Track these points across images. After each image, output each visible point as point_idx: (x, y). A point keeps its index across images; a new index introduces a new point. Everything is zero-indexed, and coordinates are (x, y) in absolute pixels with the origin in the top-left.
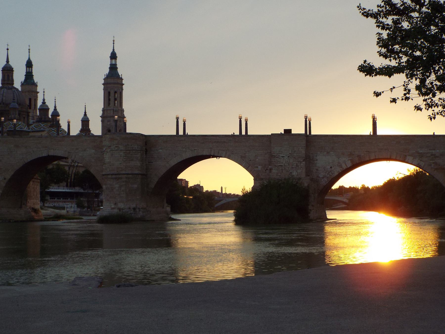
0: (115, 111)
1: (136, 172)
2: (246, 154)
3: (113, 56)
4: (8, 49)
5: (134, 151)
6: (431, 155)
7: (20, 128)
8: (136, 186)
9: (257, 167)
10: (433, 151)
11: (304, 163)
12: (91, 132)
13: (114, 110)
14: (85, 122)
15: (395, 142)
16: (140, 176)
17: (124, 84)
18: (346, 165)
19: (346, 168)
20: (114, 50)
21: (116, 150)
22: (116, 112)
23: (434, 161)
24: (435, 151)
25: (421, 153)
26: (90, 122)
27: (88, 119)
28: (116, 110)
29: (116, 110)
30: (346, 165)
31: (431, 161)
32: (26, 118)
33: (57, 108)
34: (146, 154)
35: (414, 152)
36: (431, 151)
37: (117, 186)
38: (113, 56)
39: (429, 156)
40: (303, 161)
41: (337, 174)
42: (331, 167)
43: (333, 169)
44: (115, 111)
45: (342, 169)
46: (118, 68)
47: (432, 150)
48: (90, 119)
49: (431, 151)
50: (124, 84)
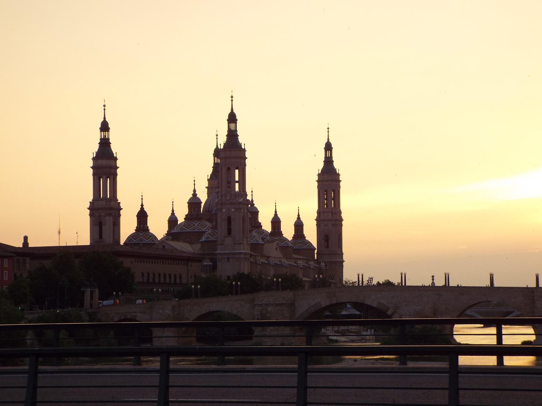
0: (334, 213)
3: (328, 147)
7: (255, 241)
12: (306, 238)
13: (332, 212)
14: (299, 226)
17: (341, 181)
20: (328, 139)
22: (335, 214)
26: (304, 226)
27: (302, 223)
28: (335, 212)
29: (335, 212)
33: (300, 217)
38: (328, 147)
44: (334, 213)
46: (334, 162)
48: (304, 224)
50: (341, 181)
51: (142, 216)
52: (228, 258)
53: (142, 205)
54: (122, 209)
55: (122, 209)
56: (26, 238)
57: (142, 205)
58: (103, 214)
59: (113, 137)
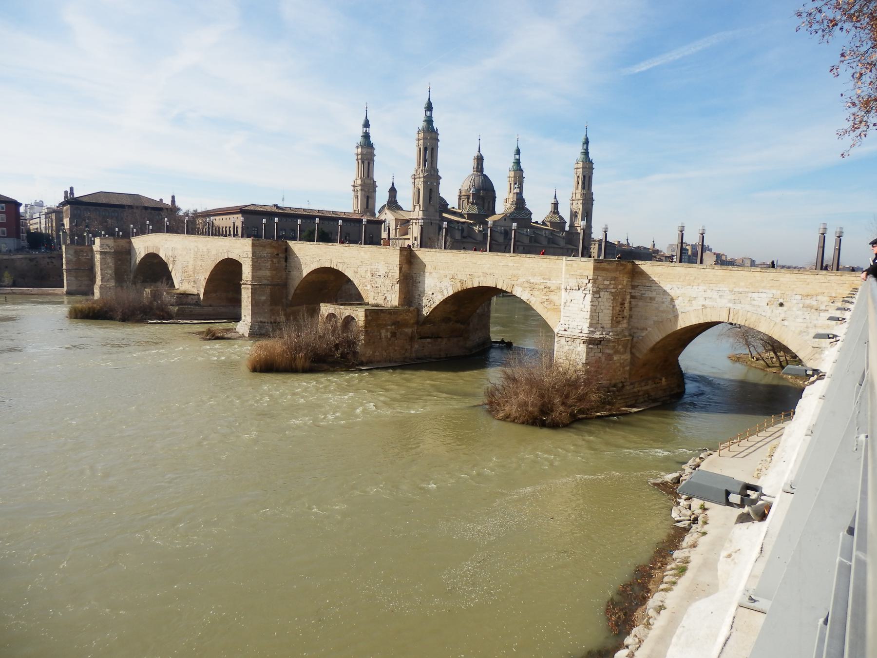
1: (265, 282)
2: (359, 269)
4: (480, 140)
5: (262, 260)
6: (545, 288)
8: (264, 298)
9: (366, 286)
10: (548, 282)
11: (398, 285)
15: (502, 264)
16: (269, 287)
18: (448, 292)
19: (448, 296)
21: (247, 258)
23: (547, 298)
24: (551, 281)
25: (533, 283)
30: (448, 292)
31: (544, 297)
32: (491, 202)
34: (286, 261)
35: (524, 280)
36: (545, 281)
37: (246, 296)
39: (543, 289)
40: (397, 283)
41: (438, 303)
42: (433, 294)
43: (434, 295)
45: (442, 296)
47: (546, 279)
49: (545, 281)
51: (393, 191)
52: (431, 223)
53: (393, 184)
54: (377, 186)
55: (377, 186)
56: (173, 197)
57: (393, 184)
59: (372, 131)
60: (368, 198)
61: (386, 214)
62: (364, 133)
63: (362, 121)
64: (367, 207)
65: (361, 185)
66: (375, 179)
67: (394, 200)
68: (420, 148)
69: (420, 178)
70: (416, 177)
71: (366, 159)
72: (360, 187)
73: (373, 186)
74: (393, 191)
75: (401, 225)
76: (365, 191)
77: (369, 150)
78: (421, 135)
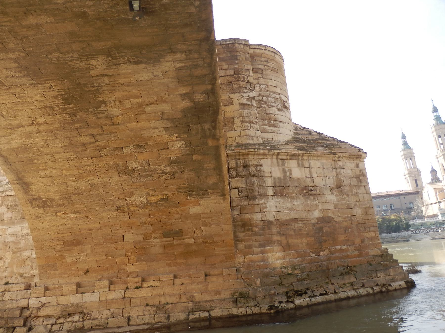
51: (433, 171)
58: (407, 177)
60: (416, 181)
61: (427, 187)
62: (403, 142)
63: (401, 136)
64: (417, 186)
65: (408, 174)
66: (418, 167)
67: (436, 177)
68: (435, 137)
69: (440, 156)
70: (438, 157)
71: (408, 157)
72: (408, 175)
73: (418, 173)
74: (433, 171)
75: (439, 192)
76: (412, 177)
77: (409, 151)
78: (434, 129)
